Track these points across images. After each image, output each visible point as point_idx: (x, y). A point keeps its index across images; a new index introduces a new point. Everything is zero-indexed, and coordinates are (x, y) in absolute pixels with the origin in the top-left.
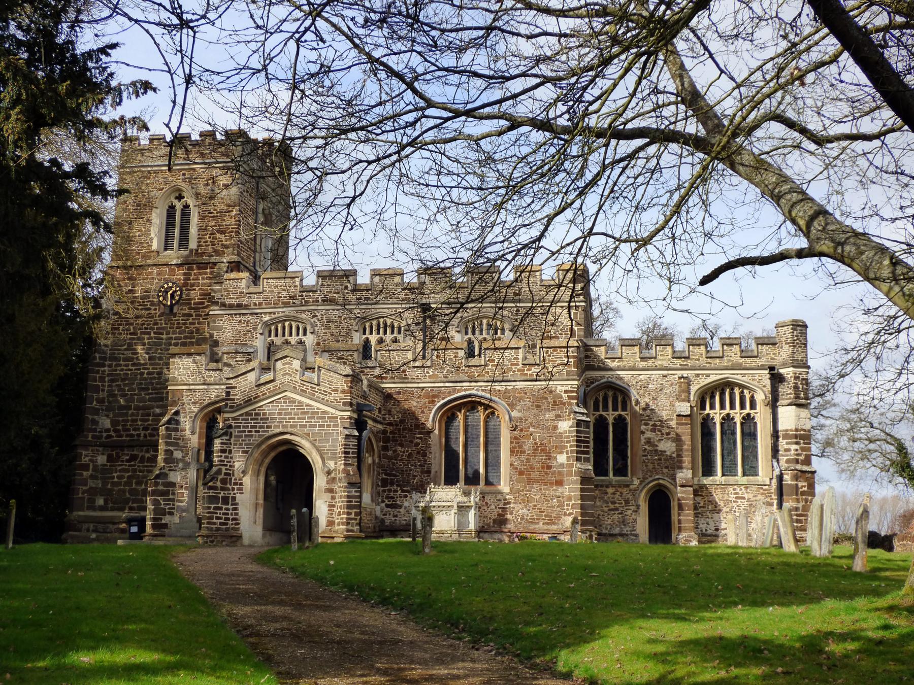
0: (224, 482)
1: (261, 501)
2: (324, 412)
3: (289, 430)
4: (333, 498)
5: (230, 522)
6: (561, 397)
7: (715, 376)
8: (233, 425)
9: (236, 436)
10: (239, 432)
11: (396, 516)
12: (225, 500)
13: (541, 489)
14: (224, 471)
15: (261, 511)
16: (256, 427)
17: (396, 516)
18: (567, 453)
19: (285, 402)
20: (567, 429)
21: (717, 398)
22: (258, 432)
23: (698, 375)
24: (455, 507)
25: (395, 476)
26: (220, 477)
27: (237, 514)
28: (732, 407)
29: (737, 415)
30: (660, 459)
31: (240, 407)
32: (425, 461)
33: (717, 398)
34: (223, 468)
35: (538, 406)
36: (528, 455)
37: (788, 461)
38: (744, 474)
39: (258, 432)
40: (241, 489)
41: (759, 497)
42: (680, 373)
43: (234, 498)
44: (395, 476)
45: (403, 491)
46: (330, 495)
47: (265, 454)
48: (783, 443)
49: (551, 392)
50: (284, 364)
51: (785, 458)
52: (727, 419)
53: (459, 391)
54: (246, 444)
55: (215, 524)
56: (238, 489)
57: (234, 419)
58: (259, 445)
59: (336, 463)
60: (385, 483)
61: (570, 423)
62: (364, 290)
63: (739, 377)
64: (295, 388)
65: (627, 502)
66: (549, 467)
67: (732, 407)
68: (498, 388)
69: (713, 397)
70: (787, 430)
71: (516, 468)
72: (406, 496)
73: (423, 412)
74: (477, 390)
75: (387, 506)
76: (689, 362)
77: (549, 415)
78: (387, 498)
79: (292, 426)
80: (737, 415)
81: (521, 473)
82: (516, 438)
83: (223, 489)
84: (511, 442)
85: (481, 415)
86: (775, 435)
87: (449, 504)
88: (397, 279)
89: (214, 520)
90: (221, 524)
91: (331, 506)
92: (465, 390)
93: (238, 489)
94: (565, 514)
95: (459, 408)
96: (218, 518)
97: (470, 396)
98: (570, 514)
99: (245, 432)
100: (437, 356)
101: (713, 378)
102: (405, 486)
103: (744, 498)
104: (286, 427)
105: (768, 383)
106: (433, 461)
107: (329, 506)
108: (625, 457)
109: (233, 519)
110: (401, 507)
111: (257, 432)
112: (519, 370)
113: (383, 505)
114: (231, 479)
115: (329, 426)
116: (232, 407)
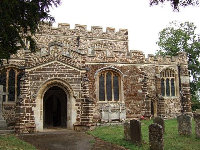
0: (26, 101)
2: (75, 70)
3: (58, 77)
4: (79, 108)
5: (29, 121)
6: (139, 70)
7: (165, 67)
8: (30, 75)
9: (31, 80)
10: (32, 78)
12: (27, 111)
13: (134, 102)
14: (26, 96)
16: (41, 76)
18: (142, 89)
19: (55, 65)
20: (142, 81)
21: (165, 73)
22: (43, 78)
23: (160, 66)
26: (25, 99)
27: (33, 117)
28: (168, 76)
29: (170, 78)
30: (151, 91)
31: (33, 67)
32: (93, 92)
33: (165, 73)
34: (26, 95)
35: (132, 73)
36: (129, 90)
37: (184, 92)
38: (172, 96)
39: (43, 78)
40: (35, 105)
41: (177, 103)
42: (156, 65)
43: (31, 109)
46: (78, 107)
47: (45, 88)
48: (183, 87)
49: (135, 68)
50: (54, 48)
51: (183, 91)
52: (167, 79)
53: (105, 66)
54: (36, 84)
55: (23, 122)
56: (33, 105)
57: (30, 72)
58: (44, 84)
59: (80, 93)
61: (143, 79)
62: (56, 30)
63: (171, 67)
64: (60, 59)
66: (136, 94)
67: (168, 76)
68: (118, 66)
69: (163, 73)
70: (184, 83)
73: (92, 73)
74: (111, 66)
76: (158, 62)
77: (136, 76)
79: (59, 76)
80: (170, 78)
81: (127, 96)
82: (125, 84)
83: (27, 105)
84: (124, 85)
85: (113, 75)
86: (180, 84)
87: (117, 109)
88: (68, 27)
89: (23, 121)
90: (26, 122)
91: (78, 112)
92: (107, 66)
93: (33, 105)
94: (142, 110)
95: (104, 72)
96: (25, 119)
97: (110, 68)
98: (144, 110)
99: (36, 78)
100: (97, 53)
101: (164, 67)
103: (173, 103)
104: (57, 76)
105: (178, 69)
107: (77, 112)
109: (31, 119)
111: (41, 78)
112: (125, 60)
114: (29, 100)
115: (76, 76)
116: (28, 66)
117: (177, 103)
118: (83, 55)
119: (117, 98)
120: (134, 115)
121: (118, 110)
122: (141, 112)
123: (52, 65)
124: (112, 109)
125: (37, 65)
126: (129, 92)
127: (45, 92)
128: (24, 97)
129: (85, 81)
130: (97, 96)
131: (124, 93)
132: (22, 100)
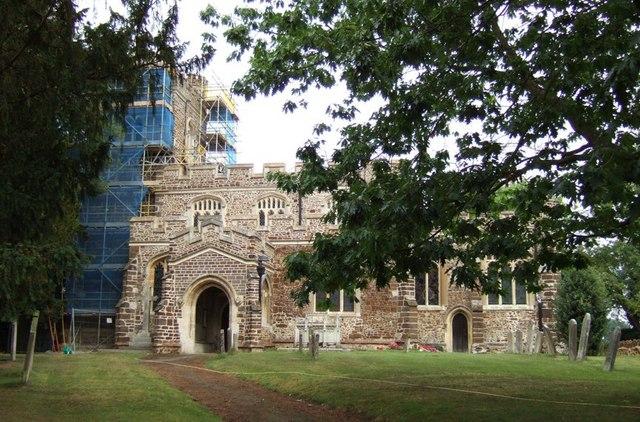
0: (168, 309)
1: (194, 323)
3: (212, 274)
4: (243, 321)
12: (170, 322)
15: (194, 329)
41: (527, 319)
43: (176, 321)
47: (196, 291)
60: (276, 310)
65: (438, 322)
66: (387, 299)
81: (368, 303)
83: (168, 314)
91: (241, 326)
108: (436, 292)
117: (527, 319)
118: (250, 237)
120: (381, 340)
122: (396, 335)
123: (205, 255)
125: (185, 256)
127: (198, 295)
128: (166, 303)
129: (250, 279)
132: (161, 307)
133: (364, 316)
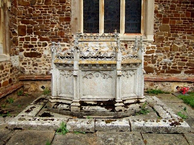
11: (36, 65)
13: (184, 38)
17: (36, 65)
24: (119, 67)
25: (33, 23)
32: (64, 7)
44: (33, 23)
45: (42, 39)
71: (160, 16)
72: (46, 45)
75: (27, 55)
78: (26, 46)
81: (165, 21)
87: (108, 61)
102: (43, 35)
106: (72, 8)
110: (39, 55)
113: (22, 54)
119: (135, 26)
120: (182, 76)
121: (109, 65)
124: (84, 62)
126: (173, 7)
130: (72, 20)
131: (156, 12)
133: (158, 39)
